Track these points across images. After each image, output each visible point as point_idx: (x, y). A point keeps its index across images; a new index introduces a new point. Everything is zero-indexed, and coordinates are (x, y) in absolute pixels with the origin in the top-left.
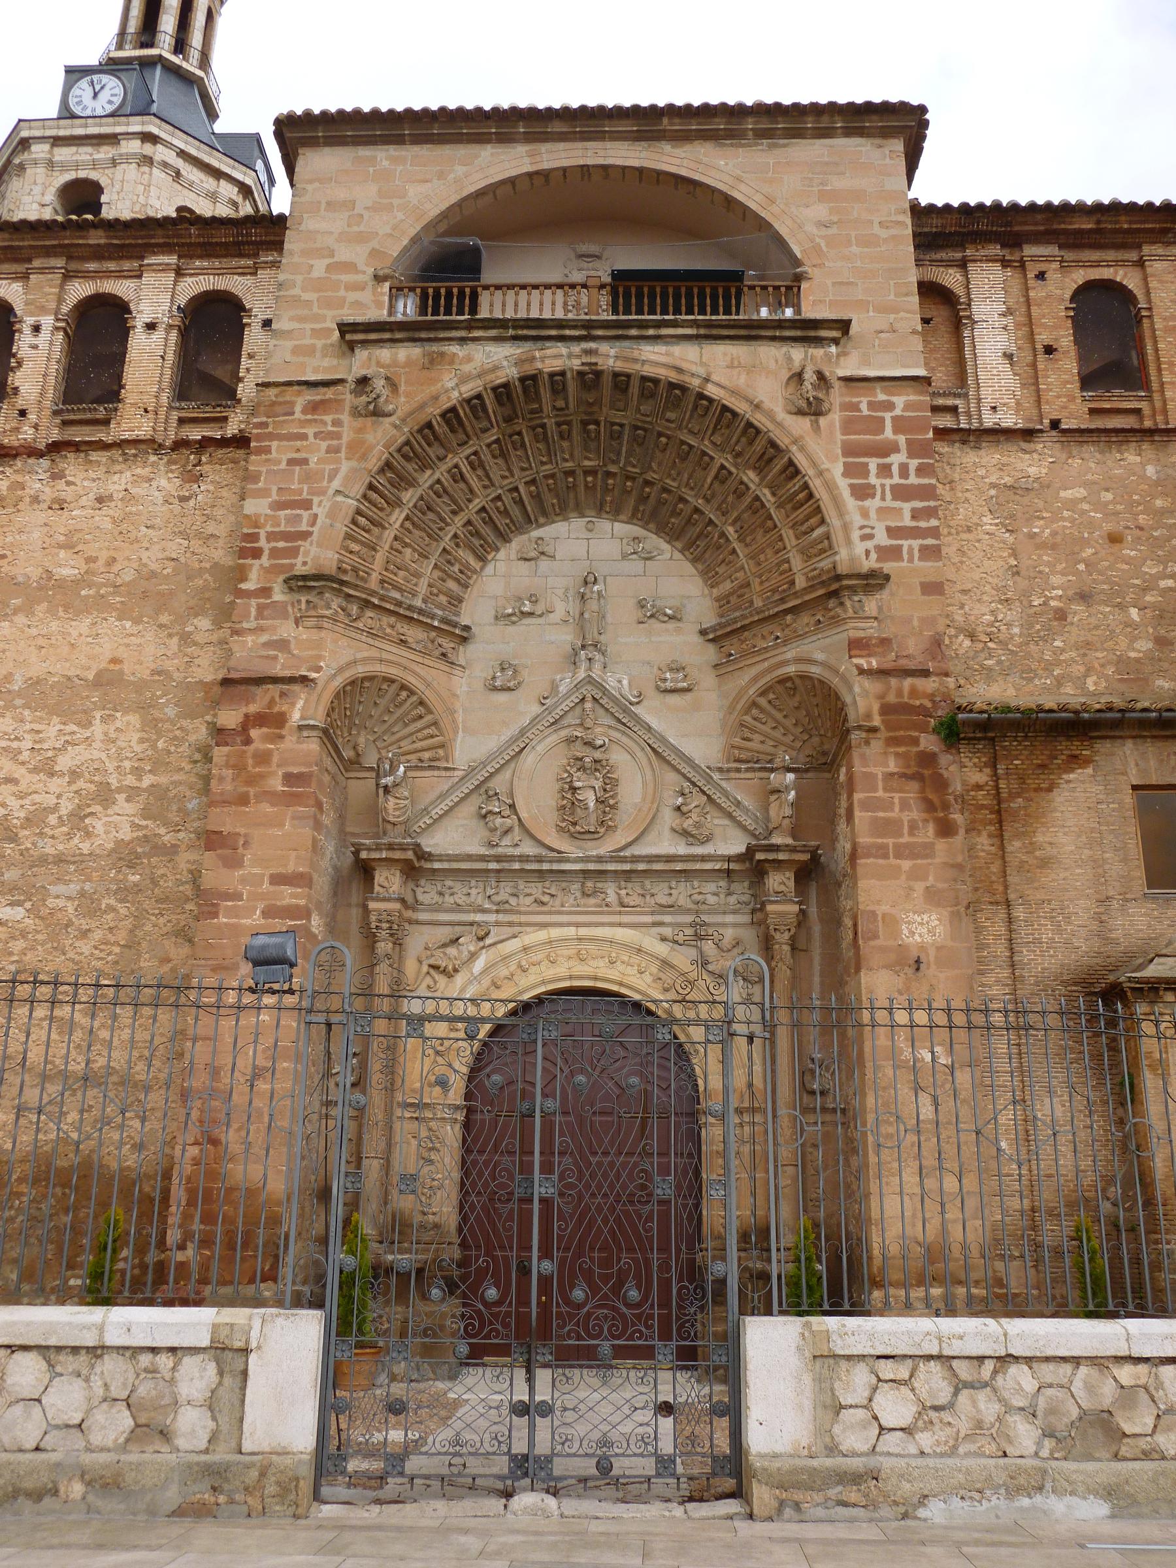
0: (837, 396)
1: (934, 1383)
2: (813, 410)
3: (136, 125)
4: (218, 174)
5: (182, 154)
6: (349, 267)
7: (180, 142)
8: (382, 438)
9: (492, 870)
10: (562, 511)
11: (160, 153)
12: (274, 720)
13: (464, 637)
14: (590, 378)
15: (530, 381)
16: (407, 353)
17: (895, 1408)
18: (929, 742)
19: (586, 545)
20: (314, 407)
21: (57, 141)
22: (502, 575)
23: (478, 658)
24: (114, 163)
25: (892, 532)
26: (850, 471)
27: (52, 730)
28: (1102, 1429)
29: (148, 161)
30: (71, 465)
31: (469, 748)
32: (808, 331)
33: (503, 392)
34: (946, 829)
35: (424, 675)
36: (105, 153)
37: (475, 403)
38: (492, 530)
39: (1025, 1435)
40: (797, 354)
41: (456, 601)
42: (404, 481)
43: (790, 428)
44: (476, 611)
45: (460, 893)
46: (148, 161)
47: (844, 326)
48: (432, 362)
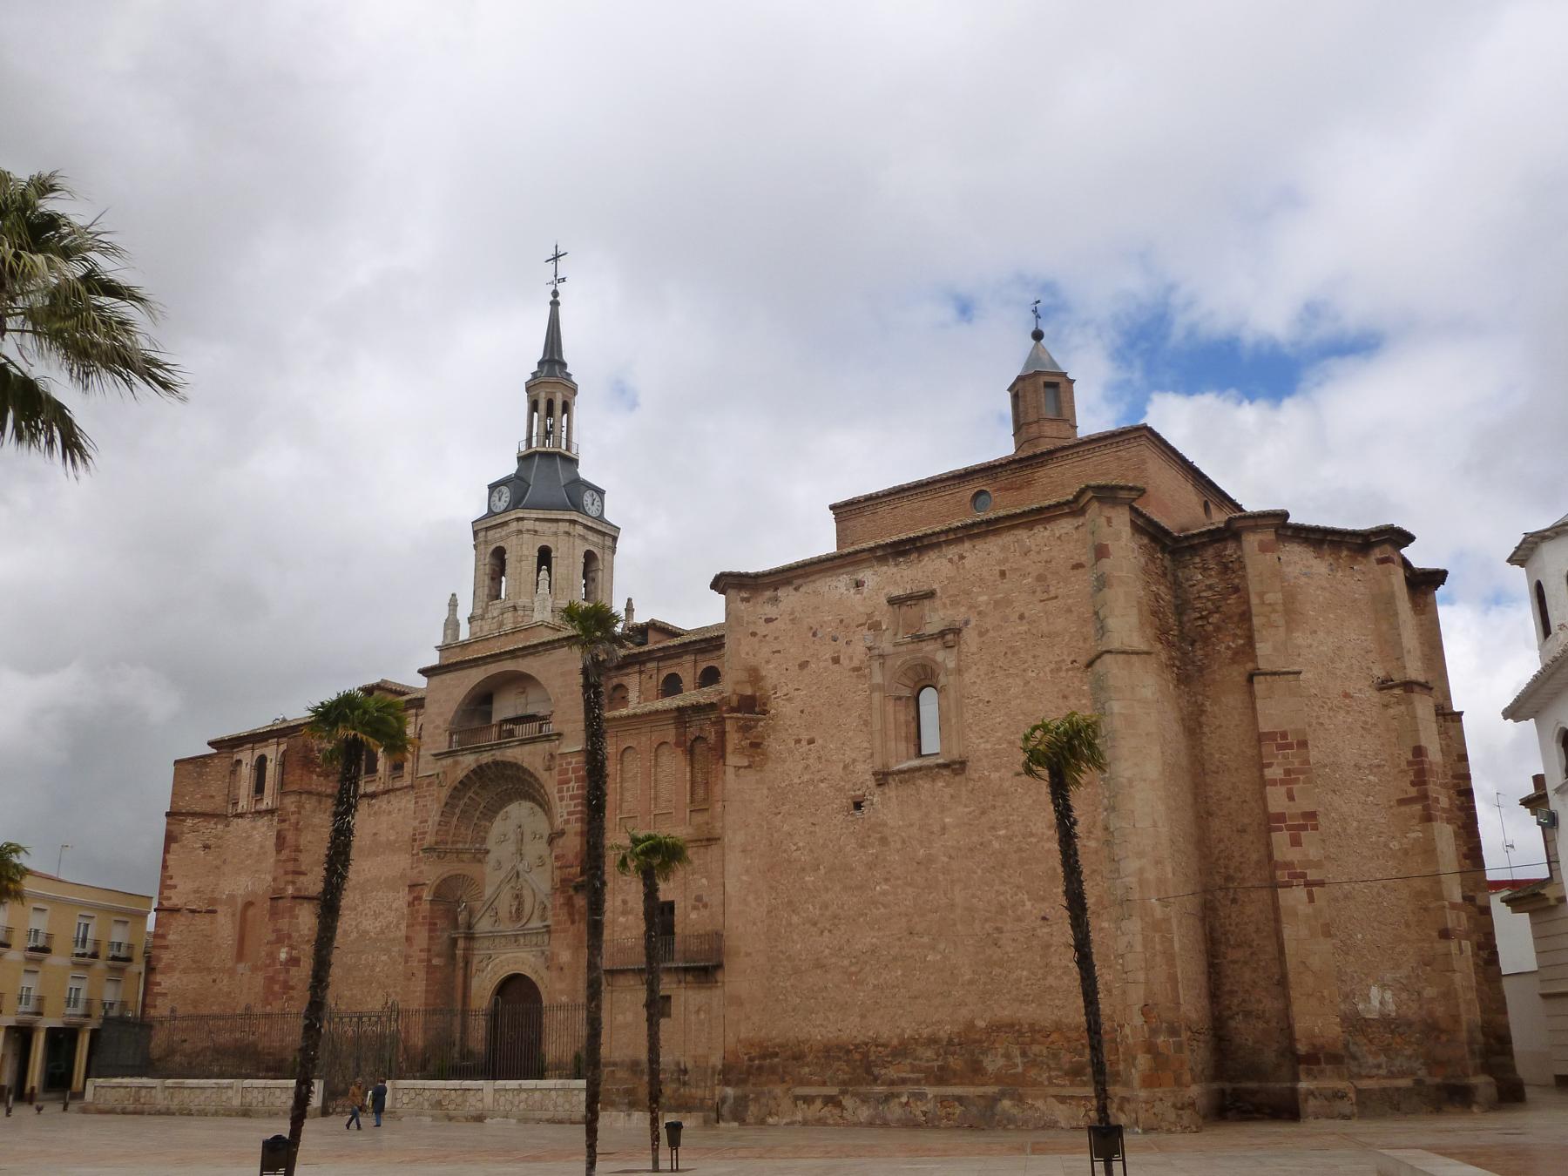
0: (557, 761)
1: (412, 1094)
2: (549, 769)
3: (513, 515)
4: (557, 521)
5: (537, 519)
6: (437, 727)
7: (535, 514)
8: (444, 793)
9: (492, 936)
10: (511, 800)
11: (527, 525)
12: (418, 898)
13: (487, 852)
14: (496, 763)
15: (480, 767)
16: (449, 761)
17: (406, 1100)
18: (571, 892)
19: (519, 811)
20: (429, 785)
21: (487, 529)
22: (498, 827)
23: (491, 858)
24: (508, 536)
25: (569, 814)
26: (560, 791)
27: (391, 895)
28: (439, 1103)
29: (520, 532)
30: (392, 796)
31: (488, 892)
32: (548, 738)
33: (474, 771)
34: (573, 922)
35: (471, 870)
36: (504, 532)
37: (467, 776)
38: (491, 812)
39: (426, 1105)
40: (547, 745)
41: (484, 840)
42: (454, 806)
43: (543, 776)
44: (490, 844)
45: (486, 943)
46: (520, 532)
47: (560, 735)
48: (456, 763)
